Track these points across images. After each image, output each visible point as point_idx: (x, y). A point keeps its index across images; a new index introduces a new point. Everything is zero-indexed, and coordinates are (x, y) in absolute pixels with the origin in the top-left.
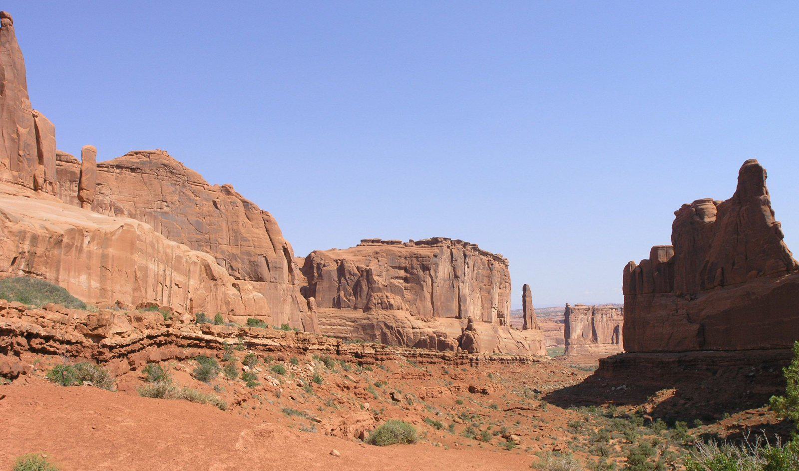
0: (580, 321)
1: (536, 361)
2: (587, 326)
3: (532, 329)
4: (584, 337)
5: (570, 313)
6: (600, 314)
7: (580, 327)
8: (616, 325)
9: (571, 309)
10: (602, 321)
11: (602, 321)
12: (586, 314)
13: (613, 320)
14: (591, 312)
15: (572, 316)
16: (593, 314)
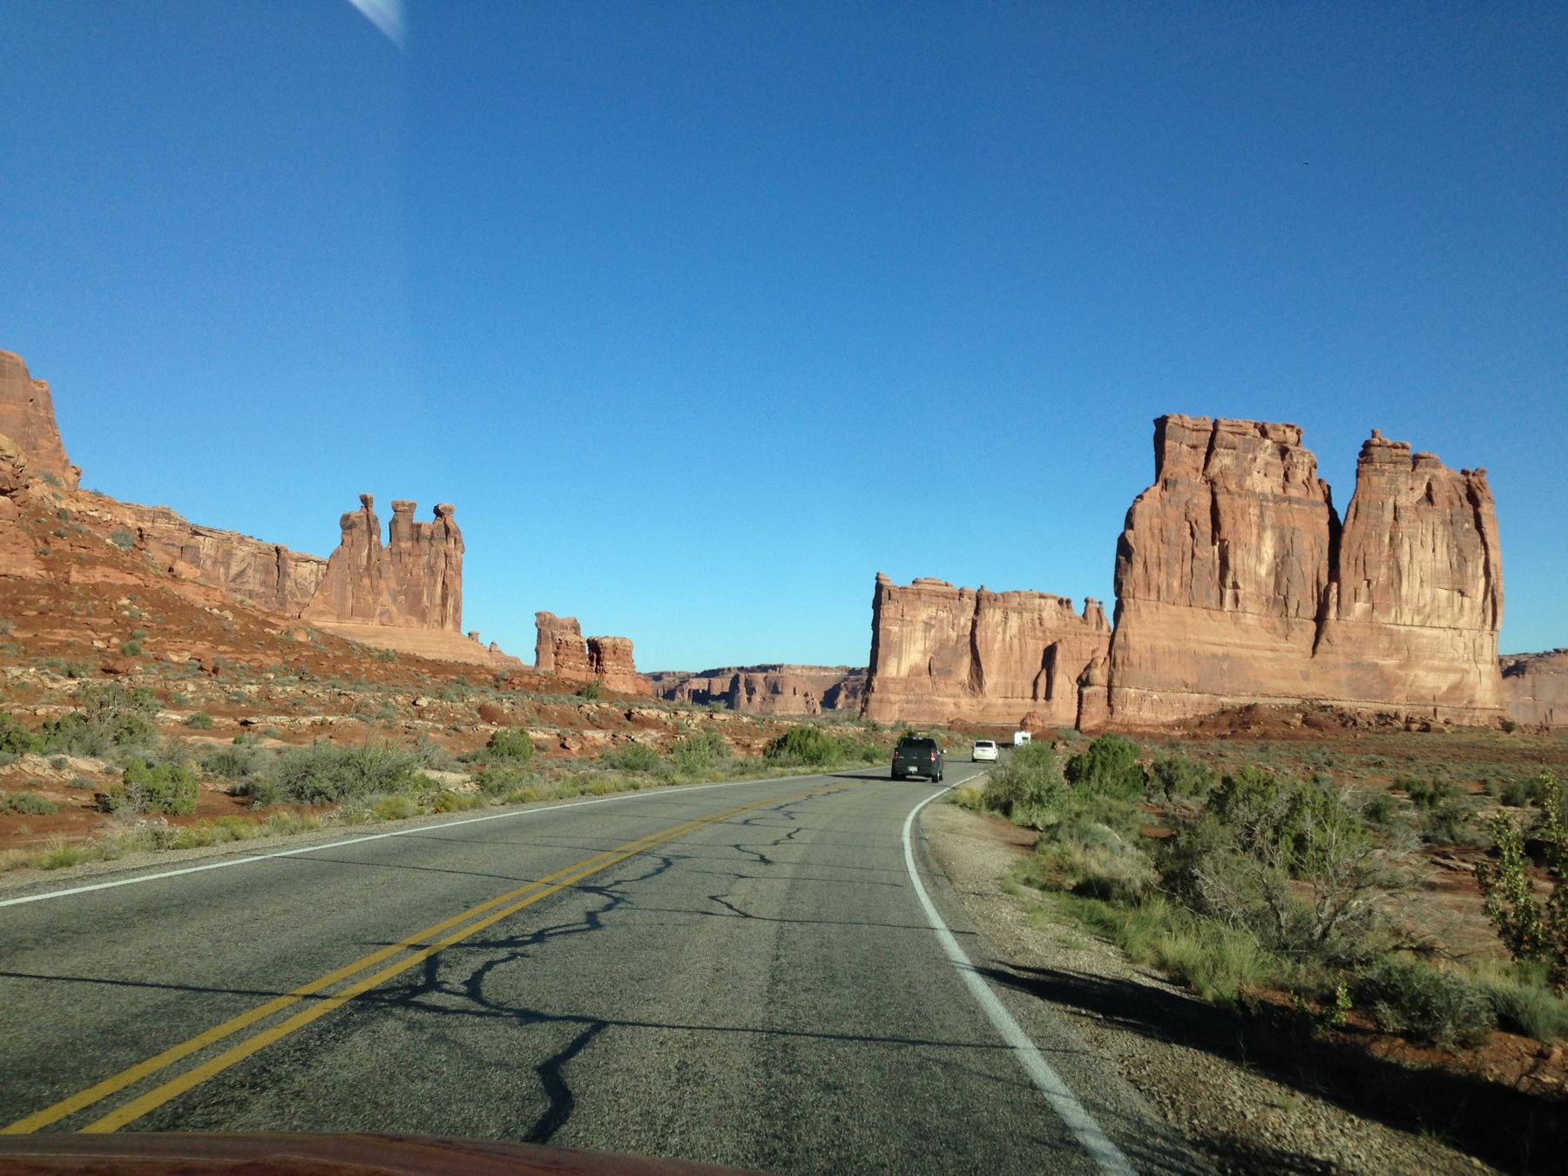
0: (920, 627)
4: (934, 673)
10: (1004, 632)
14: (970, 604)
15: (888, 610)
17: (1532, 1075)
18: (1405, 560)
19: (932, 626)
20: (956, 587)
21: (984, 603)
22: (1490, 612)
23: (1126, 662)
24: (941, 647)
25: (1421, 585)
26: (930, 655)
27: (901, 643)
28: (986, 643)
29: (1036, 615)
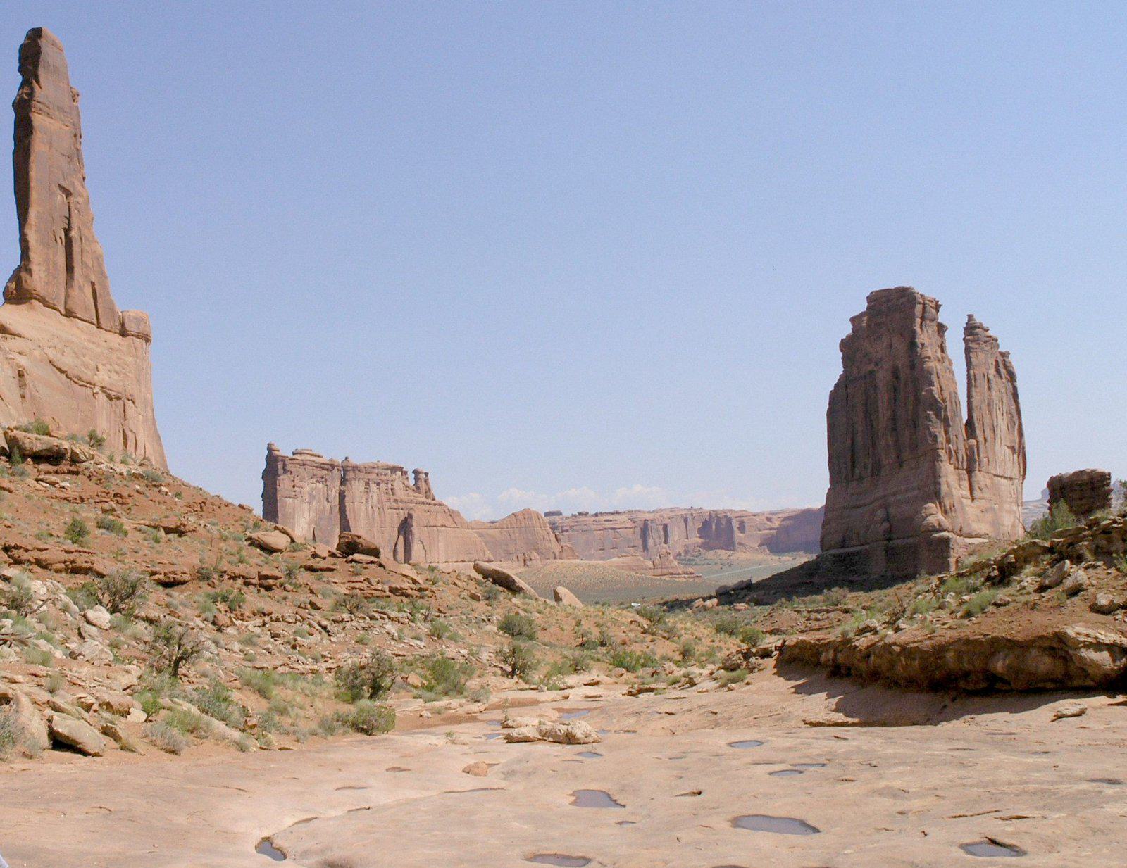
0: (307, 497)
1: (38, 458)
2: (327, 513)
3: (69, 314)
5: (280, 471)
6: (362, 483)
7: (306, 514)
8: (403, 514)
9: (283, 459)
10: (367, 501)
11: (367, 501)
12: (323, 480)
13: (396, 501)
14: (337, 475)
15: (284, 482)
16: (343, 481)
17: (1078, 815)
18: (995, 424)
19: (314, 497)
20: (325, 459)
21: (350, 475)
22: (1022, 465)
23: (953, 508)
24: (320, 518)
25: (1001, 443)
26: (313, 526)
27: (294, 513)
28: (354, 510)
29: (390, 485)
